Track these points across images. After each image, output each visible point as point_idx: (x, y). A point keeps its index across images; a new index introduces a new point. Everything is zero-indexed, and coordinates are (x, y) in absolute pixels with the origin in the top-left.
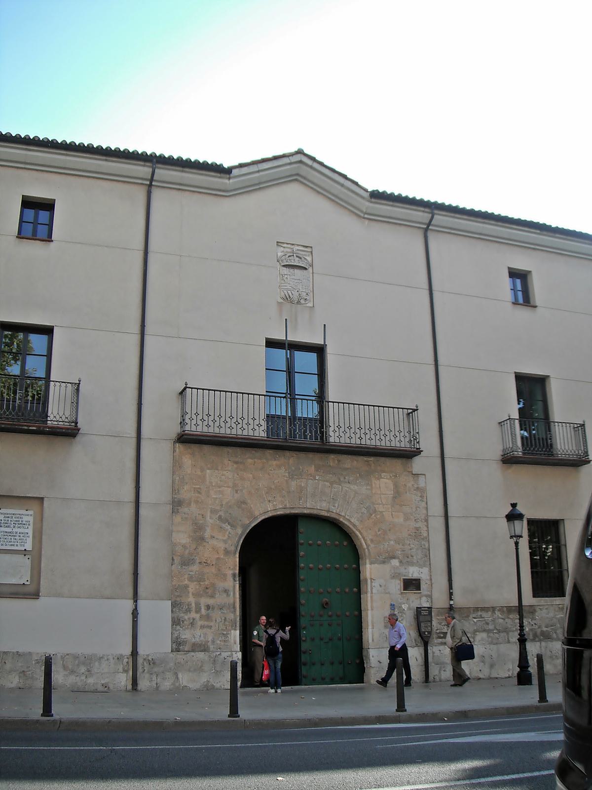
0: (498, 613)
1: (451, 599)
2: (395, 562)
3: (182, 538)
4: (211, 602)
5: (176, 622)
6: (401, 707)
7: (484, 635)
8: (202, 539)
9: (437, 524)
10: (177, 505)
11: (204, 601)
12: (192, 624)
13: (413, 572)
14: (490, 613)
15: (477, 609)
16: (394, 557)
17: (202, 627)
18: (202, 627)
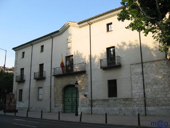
0: (101, 101)
1: (91, 98)
2: (83, 92)
3: (56, 90)
4: (59, 100)
5: (55, 103)
6: (15, 115)
7: (98, 105)
8: (58, 90)
9: (90, 84)
10: (55, 86)
11: (58, 100)
12: (57, 103)
13: (86, 93)
14: (99, 101)
15: (97, 100)
16: (83, 91)
17: (58, 103)
18: (58, 103)
